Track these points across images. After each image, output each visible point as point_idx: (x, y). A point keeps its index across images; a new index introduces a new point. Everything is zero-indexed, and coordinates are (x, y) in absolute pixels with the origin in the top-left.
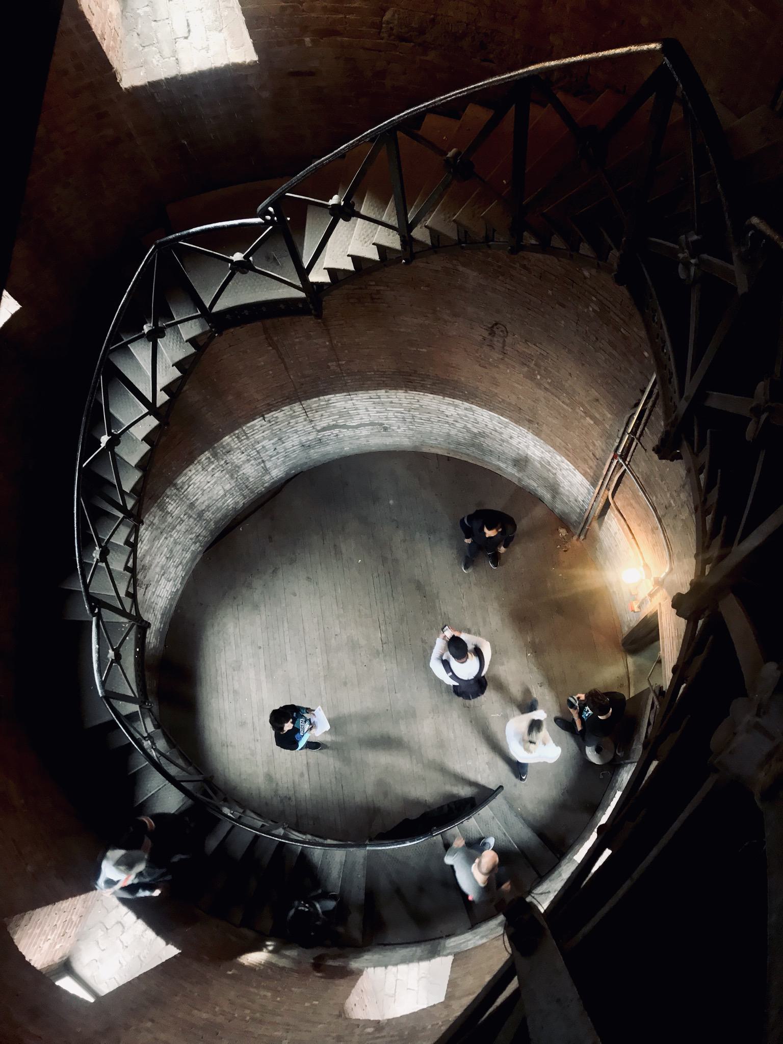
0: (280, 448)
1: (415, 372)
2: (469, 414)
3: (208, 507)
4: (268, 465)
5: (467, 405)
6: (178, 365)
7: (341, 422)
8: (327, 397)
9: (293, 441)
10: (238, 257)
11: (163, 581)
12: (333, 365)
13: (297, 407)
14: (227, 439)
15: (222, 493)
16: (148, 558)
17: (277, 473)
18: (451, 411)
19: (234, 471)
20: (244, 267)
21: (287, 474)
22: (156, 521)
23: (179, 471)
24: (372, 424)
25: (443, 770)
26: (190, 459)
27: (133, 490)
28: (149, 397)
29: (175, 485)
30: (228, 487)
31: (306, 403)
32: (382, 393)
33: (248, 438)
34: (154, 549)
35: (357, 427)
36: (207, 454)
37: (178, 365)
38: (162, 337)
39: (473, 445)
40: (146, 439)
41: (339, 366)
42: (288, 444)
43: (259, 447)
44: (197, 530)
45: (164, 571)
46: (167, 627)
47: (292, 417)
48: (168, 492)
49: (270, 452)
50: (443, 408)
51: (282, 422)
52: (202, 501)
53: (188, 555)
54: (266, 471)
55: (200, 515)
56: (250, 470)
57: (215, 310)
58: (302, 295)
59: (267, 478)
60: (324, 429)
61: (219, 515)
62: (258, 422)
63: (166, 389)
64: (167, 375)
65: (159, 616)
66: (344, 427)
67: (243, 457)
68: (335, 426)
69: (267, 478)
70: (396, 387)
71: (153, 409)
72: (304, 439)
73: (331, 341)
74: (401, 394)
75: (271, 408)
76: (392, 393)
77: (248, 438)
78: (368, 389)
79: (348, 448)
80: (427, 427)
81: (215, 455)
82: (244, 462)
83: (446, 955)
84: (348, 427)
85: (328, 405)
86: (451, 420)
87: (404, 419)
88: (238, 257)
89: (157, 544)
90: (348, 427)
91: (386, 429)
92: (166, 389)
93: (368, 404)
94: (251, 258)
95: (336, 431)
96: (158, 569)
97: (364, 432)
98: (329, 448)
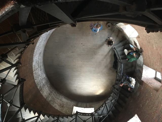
0: (40, 75)
1: (32, 48)
2: (42, 37)
3: (50, 91)
4: (43, 78)
5: (40, 38)
6: (30, 112)
7: (37, 63)
8: (33, 66)
9: (40, 73)
10: (9, 105)
11: (62, 100)
12: (27, 65)
13: (34, 73)
14: (38, 88)
15: (47, 88)
16: (59, 104)
17: (44, 76)
18: (40, 40)
19: (44, 85)
20: (11, 103)
21: (45, 73)
22: (52, 102)
23: (44, 98)
24: (39, 56)
25: (106, 56)
26: (42, 96)
27: (53, 118)
28: (36, 118)
29: (46, 99)
30: (46, 86)
31: (33, 70)
32: (34, 54)
33: (38, 83)
34: (57, 103)
35: (39, 59)
36: (41, 92)
37: (30, 112)
38: (24, 119)
39: (47, 36)
40: (44, 116)
41: (28, 64)
42: (40, 74)
43: (40, 80)
44: (54, 93)
45: (61, 100)
46: (70, 99)
47: (36, 73)
48: (47, 100)
49: (41, 77)
50: (40, 42)
51: (36, 75)
52: (49, 92)
53: (58, 94)
54: (44, 78)
55: (51, 92)
56: (44, 82)
57: (20, 106)
58: (19, 86)
59: (45, 78)
60: (38, 66)
61: (51, 88)
62: (36, 81)
63: (35, 114)
64: (32, 115)
65: (68, 101)
66: (38, 62)
67: (42, 83)
68: (38, 64)
69: (45, 78)
70: (34, 51)
71: (38, 117)
72: (39, 70)
73: (23, 66)
74: (35, 50)
75: (34, 78)
76: (34, 52)
77: (38, 83)
78: (33, 57)
79: (42, 61)
80: (42, 45)
81: (41, 90)
82: (43, 83)
83: (143, 66)
84: (39, 61)
85: (34, 66)
86: (42, 40)
87: (39, 50)
88: (9, 105)
89: (56, 102)
90: (39, 61)
91: (40, 53)
92: (35, 114)
93: (35, 57)
94: (9, 101)
95: (39, 63)
96: (60, 101)
97: (40, 58)
98: (42, 65)
